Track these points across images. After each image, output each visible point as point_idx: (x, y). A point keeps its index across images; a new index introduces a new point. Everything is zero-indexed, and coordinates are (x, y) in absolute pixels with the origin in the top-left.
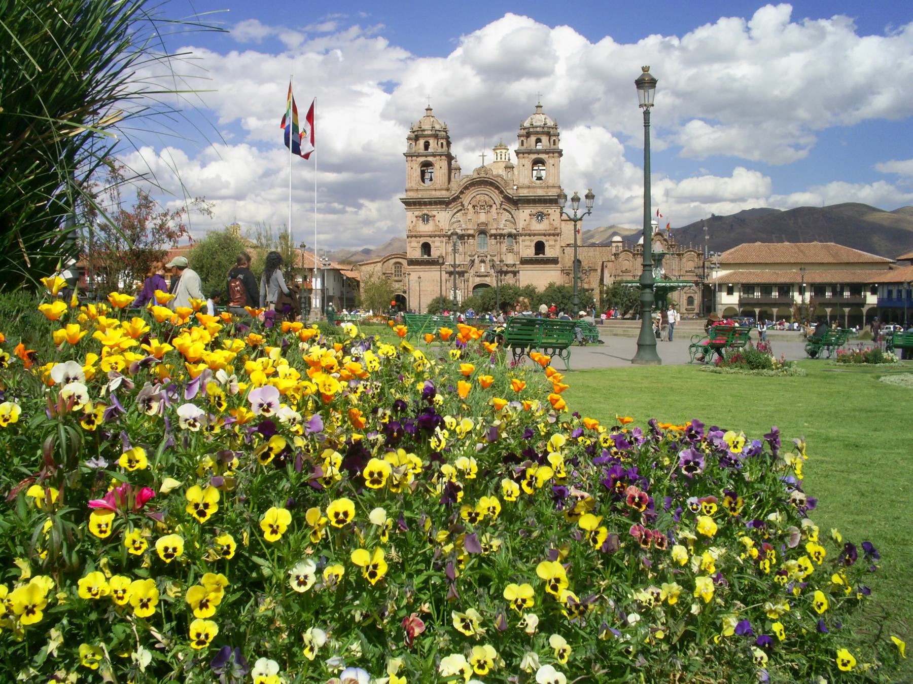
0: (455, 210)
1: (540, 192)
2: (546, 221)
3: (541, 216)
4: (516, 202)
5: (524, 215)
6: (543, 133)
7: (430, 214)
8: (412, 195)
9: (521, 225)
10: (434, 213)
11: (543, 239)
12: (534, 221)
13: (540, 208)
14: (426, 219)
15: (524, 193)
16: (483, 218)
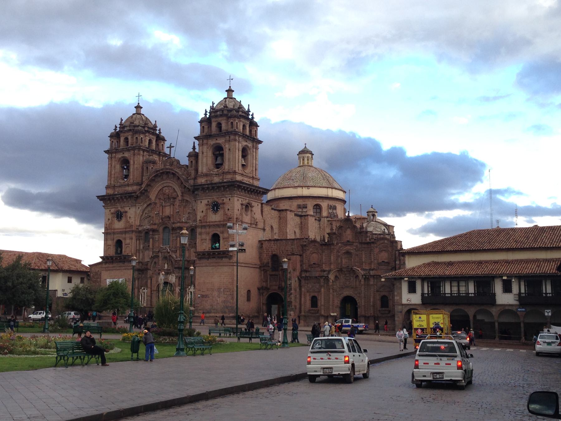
0: (145, 205)
1: (216, 180)
2: (221, 212)
3: (216, 207)
4: (196, 190)
5: (201, 206)
6: (221, 116)
7: (122, 210)
8: (111, 192)
9: (199, 216)
10: (127, 209)
11: (218, 231)
12: (210, 213)
13: (215, 197)
14: (119, 216)
15: (202, 181)
16: (168, 211)
